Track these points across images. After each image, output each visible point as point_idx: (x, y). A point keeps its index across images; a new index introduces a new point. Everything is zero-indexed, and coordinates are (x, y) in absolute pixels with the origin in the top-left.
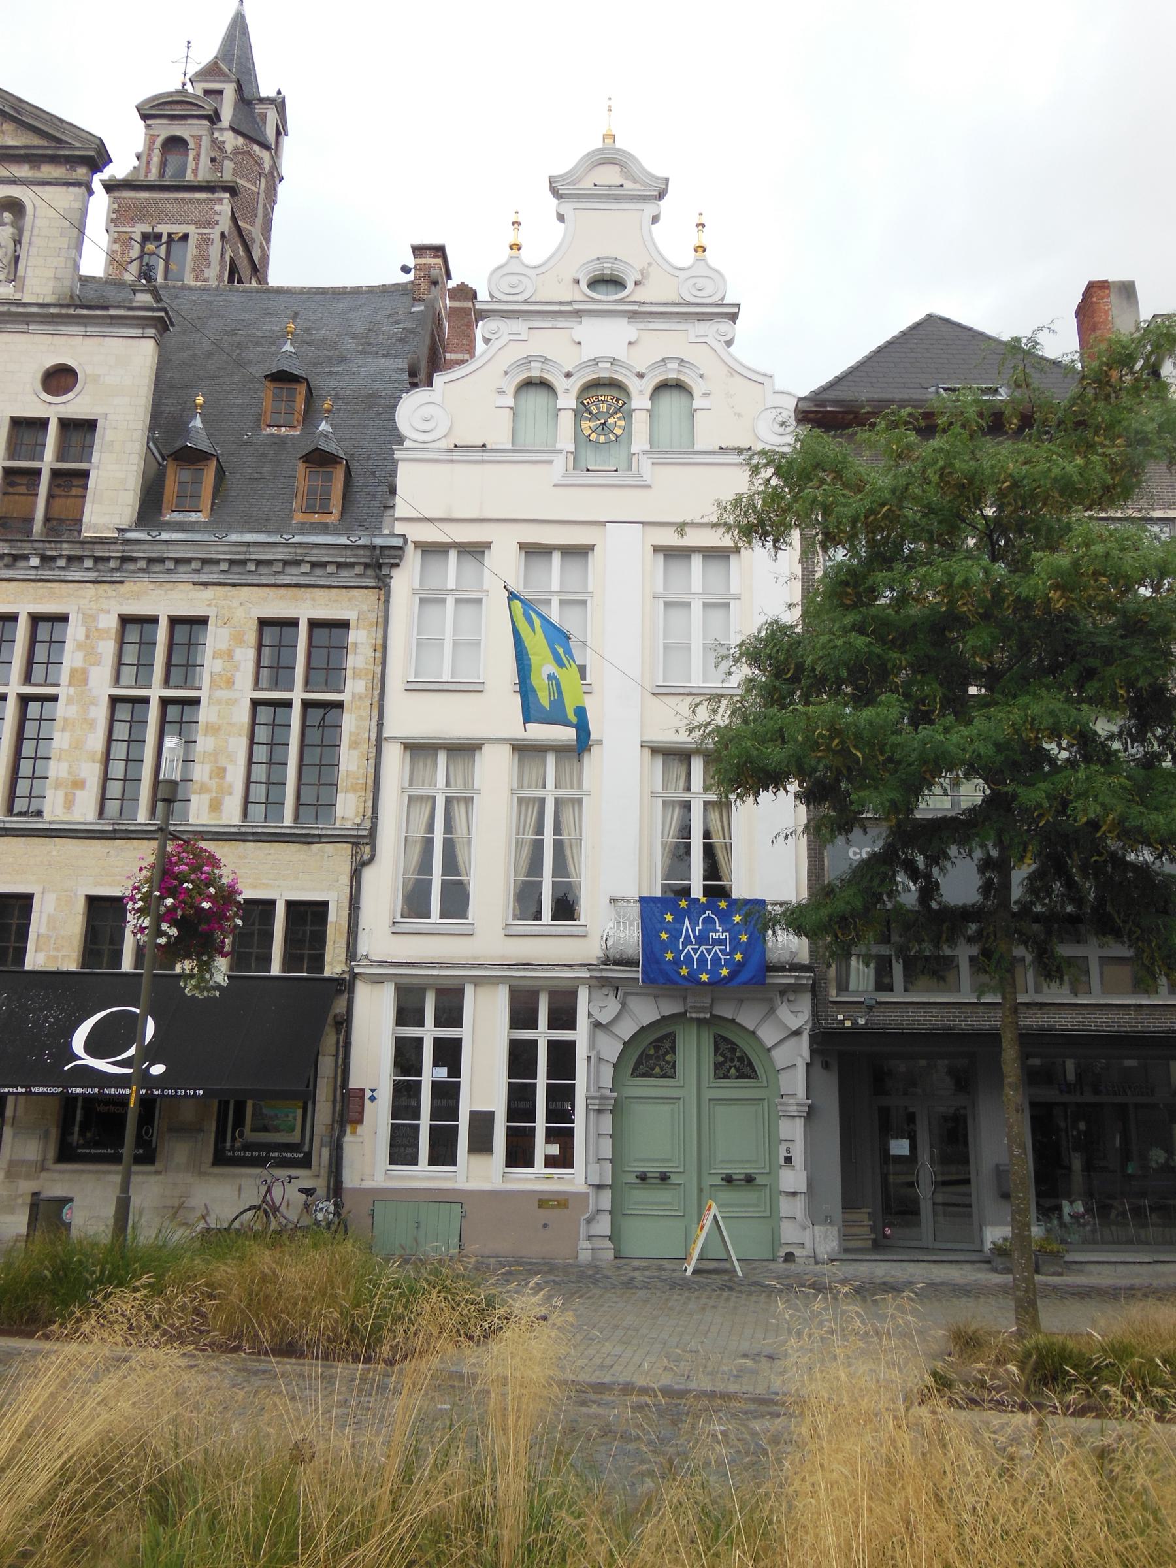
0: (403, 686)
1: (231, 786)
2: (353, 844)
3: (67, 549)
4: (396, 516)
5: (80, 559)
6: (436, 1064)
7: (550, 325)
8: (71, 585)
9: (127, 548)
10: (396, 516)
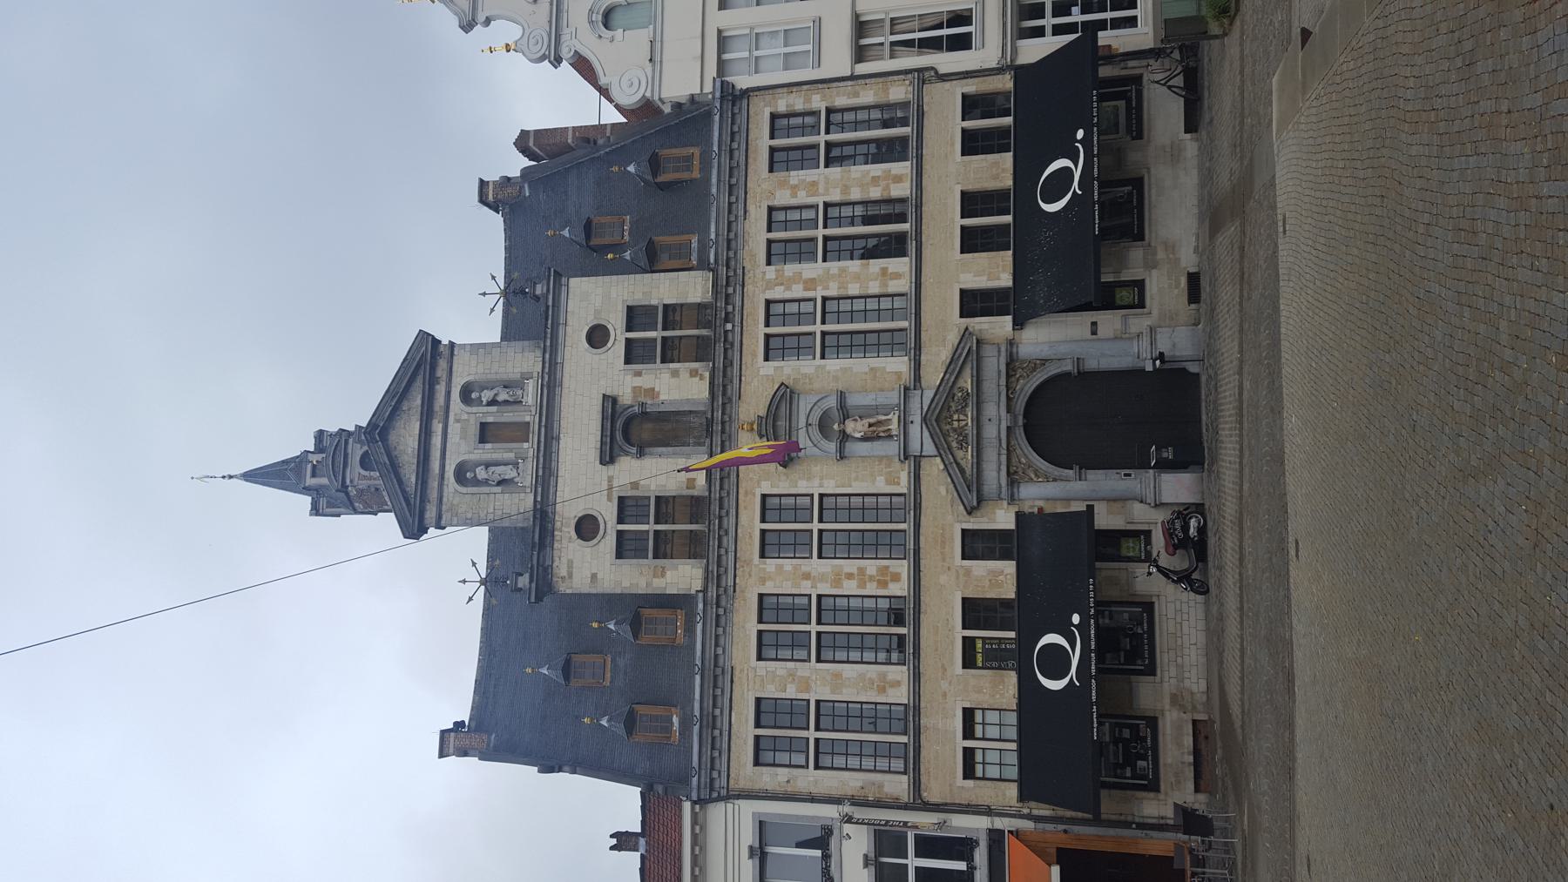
0: (816, 70)
1: (884, 171)
2: (923, 84)
3: (721, 304)
4: (698, 91)
5: (727, 296)
6: (1070, 14)
7: (565, 15)
8: (745, 302)
9: (720, 263)
10: (698, 91)
